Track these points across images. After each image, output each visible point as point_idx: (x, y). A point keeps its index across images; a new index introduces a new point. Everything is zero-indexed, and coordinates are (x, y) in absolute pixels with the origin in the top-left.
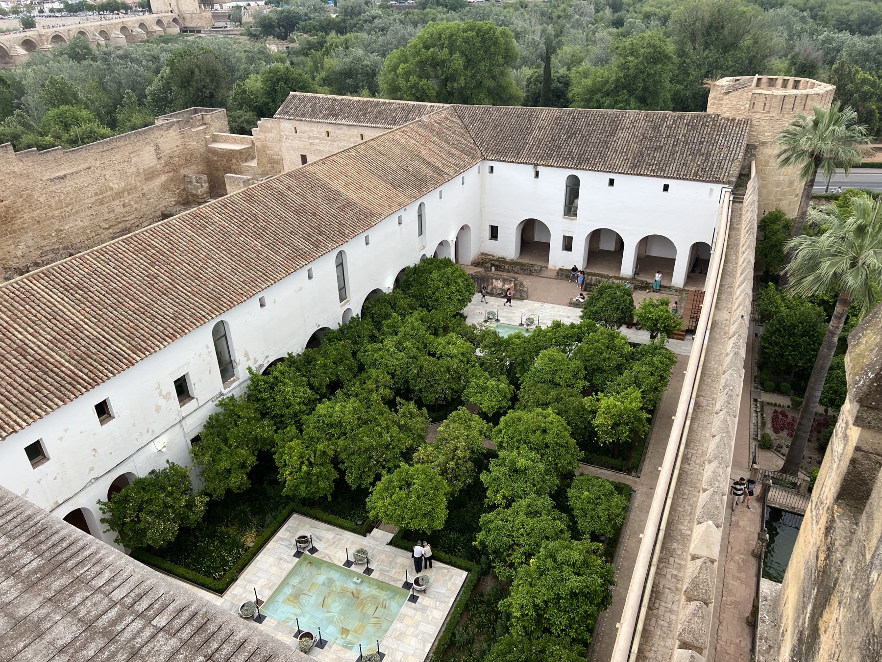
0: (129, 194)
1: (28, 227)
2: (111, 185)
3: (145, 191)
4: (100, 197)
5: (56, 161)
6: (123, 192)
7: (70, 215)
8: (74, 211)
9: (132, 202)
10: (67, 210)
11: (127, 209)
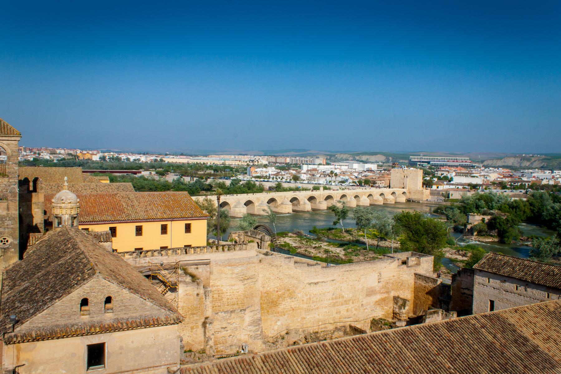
0: (353, 303)
1: (286, 312)
2: (343, 294)
3: (364, 303)
4: (335, 301)
5: (316, 272)
6: (350, 300)
7: (312, 310)
8: (316, 307)
9: (353, 310)
10: (313, 305)
11: (349, 313)
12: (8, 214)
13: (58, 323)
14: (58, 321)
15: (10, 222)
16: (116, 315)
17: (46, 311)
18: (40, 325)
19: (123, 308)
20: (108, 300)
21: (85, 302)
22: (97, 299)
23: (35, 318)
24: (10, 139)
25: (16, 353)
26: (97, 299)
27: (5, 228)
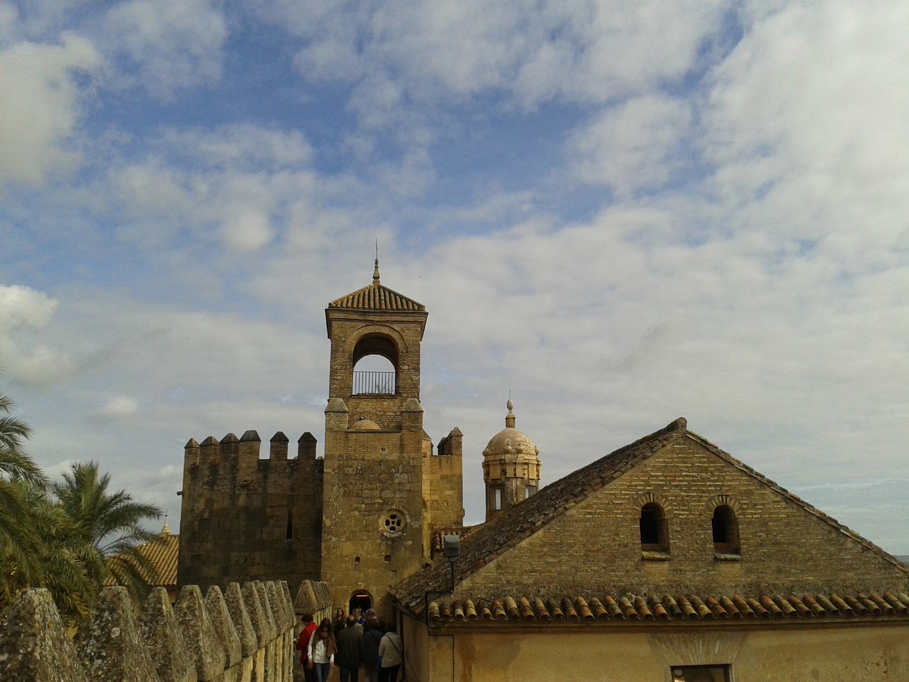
12: (401, 458)
13: (578, 578)
14: (577, 569)
15: (405, 476)
16: (750, 571)
17: (540, 533)
18: (528, 580)
19: (773, 550)
20: (723, 525)
21: (652, 526)
22: (687, 518)
23: (508, 554)
24: (406, 319)
25: (459, 667)
26: (687, 518)
27: (394, 492)
